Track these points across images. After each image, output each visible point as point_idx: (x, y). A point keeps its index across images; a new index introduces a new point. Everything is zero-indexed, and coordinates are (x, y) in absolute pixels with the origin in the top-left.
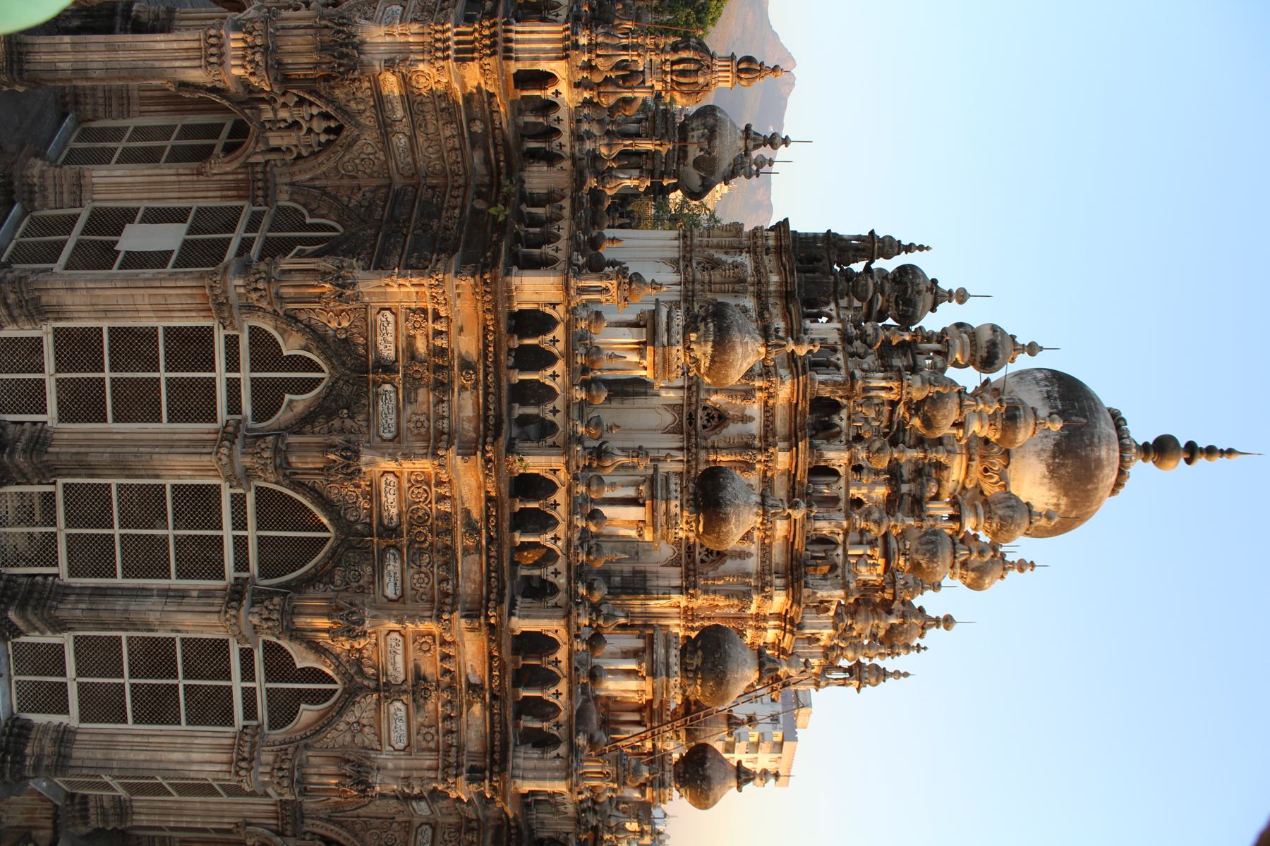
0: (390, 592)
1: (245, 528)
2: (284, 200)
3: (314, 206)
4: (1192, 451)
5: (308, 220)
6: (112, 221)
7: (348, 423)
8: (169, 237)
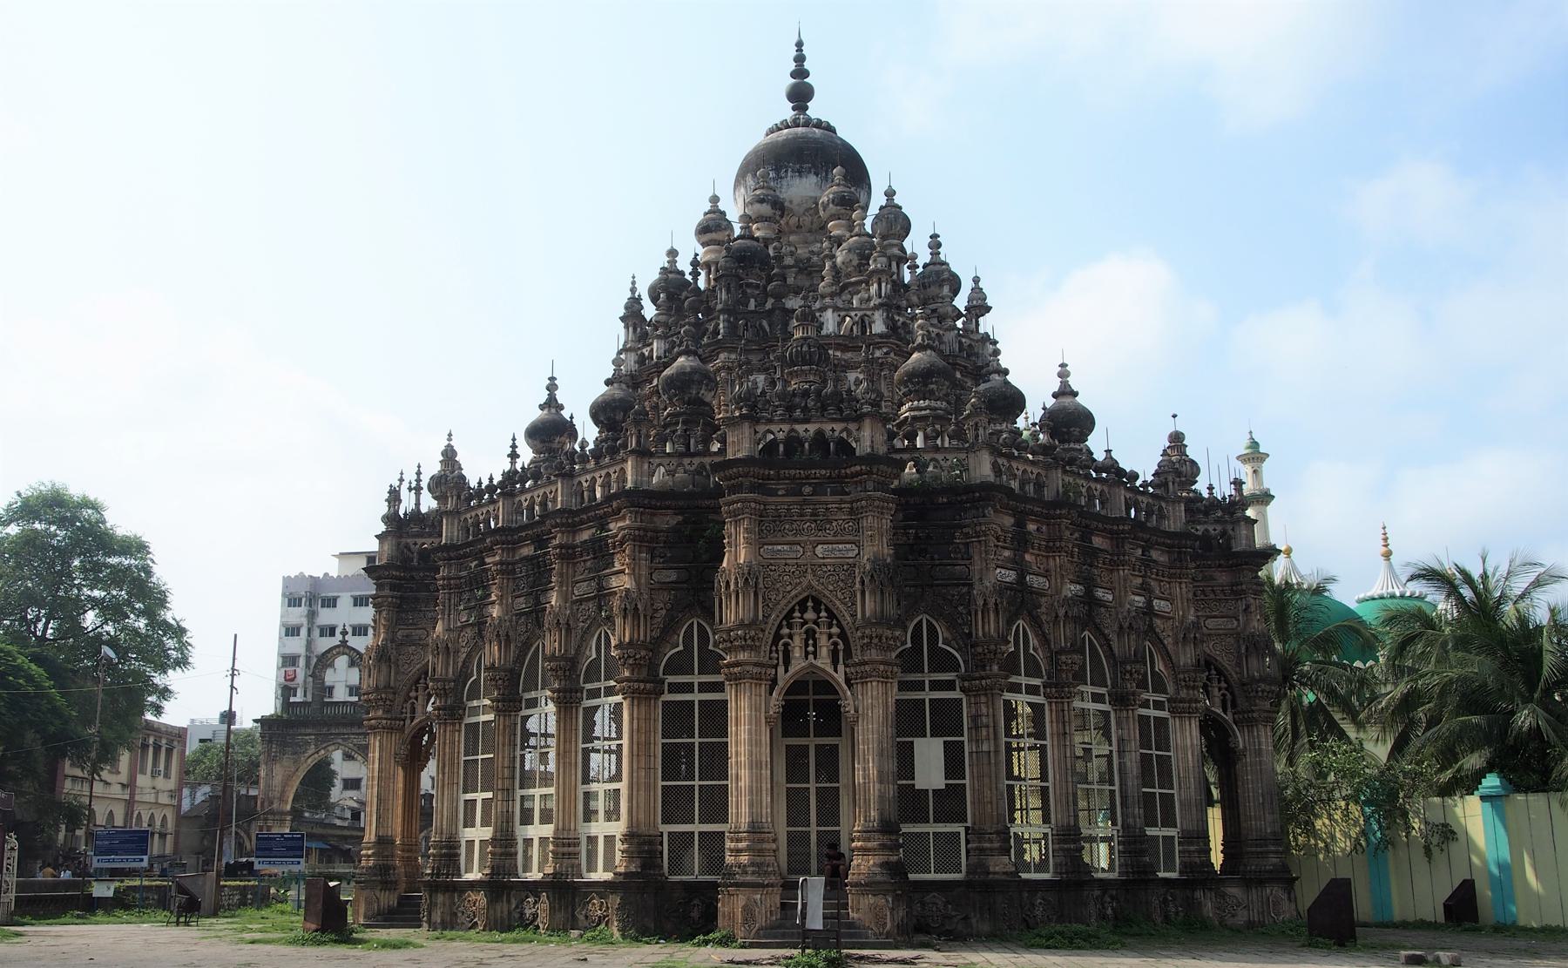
0: (1110, 598)
4: (800, 73)
7: (1043, 609)
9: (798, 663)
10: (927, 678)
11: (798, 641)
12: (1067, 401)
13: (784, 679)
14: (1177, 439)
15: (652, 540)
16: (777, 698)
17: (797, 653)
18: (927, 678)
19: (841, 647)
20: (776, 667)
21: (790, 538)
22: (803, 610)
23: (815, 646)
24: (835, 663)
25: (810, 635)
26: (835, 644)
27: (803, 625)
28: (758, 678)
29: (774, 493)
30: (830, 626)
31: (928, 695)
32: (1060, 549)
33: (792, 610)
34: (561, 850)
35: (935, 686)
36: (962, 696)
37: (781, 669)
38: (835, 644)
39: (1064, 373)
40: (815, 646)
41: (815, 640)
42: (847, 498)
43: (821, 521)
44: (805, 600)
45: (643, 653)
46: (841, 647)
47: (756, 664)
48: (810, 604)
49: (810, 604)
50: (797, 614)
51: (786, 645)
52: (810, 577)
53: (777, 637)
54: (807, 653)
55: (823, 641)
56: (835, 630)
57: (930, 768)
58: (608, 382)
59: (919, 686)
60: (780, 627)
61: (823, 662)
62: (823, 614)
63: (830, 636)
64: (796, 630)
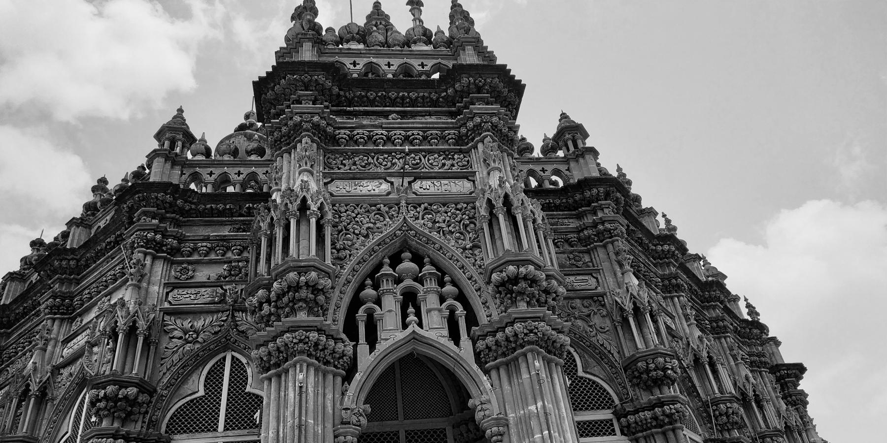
9: (392, 333)
11: (391, 303)
23: (418, 314)
24: (455, 336)
25: (410, 300)
26: (452, 311)
27: (398, 281)
30: (442, 284)
33: (380, 266)
37: (363, 347)
40: (418, 314)
46: (460, 310)
48: (407, 254)
50: (386, 270)
51: (370, 315)
53: (356, 303)
54: (405, 326)
60: (362, 287)
62: (428, 268)
63: (442, 300)
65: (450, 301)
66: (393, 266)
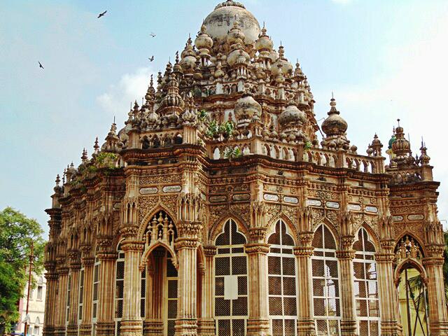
0: (338, 206)
1: (322, 252)
2: (214, 243)
3: (217, 232)
5: (223, 232)
6: (222, 306)
8: (231, 282)
10: (231, 247)
11: (154, 232)
12: (335, 117)
13: (147, 247)
14: (399, 132)
15: (114, 190)
16: (144, 258)
17: (154, 237)
18: (231, 247)
19: (173, 234)
20: (144, 244)
21: (152, 185)
22: (158, 217)
24: (170, 241)
25: (160, 228)
26: (171, 232)
28: (136, 249)
29: (146, 164)
30: (169, 224)
31: (231, 255)
32: (303, 184)
33: (153, 218)
34: (83, 330)
35: (235, 251)
36: (247, 255)
38: (171, 232)
39: (333, 102)
41: (162, 231)
42: (176, 164)
43: (165, 175)
44: (159, 212)
45: (106, 240)
46: (173, 234)
47: (133, 243)
48: (161, 214)
49: (161, 214)
50: (155, 219)
52: (160, 201)
53: (147, 230)
54: (159, 237)
55: (165, 231)
56: (171, 226)
57: (231, 293)
58: (126, 123)
59: (227, 251)
61: (165, 241)
62: (166, 218)
63: (169, 228)
64: (154, 227)
65: (171, 230)
66: (157, 218)
